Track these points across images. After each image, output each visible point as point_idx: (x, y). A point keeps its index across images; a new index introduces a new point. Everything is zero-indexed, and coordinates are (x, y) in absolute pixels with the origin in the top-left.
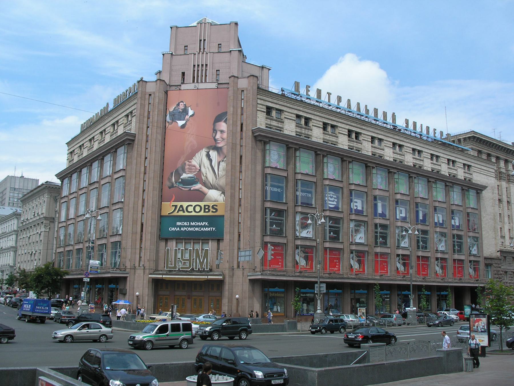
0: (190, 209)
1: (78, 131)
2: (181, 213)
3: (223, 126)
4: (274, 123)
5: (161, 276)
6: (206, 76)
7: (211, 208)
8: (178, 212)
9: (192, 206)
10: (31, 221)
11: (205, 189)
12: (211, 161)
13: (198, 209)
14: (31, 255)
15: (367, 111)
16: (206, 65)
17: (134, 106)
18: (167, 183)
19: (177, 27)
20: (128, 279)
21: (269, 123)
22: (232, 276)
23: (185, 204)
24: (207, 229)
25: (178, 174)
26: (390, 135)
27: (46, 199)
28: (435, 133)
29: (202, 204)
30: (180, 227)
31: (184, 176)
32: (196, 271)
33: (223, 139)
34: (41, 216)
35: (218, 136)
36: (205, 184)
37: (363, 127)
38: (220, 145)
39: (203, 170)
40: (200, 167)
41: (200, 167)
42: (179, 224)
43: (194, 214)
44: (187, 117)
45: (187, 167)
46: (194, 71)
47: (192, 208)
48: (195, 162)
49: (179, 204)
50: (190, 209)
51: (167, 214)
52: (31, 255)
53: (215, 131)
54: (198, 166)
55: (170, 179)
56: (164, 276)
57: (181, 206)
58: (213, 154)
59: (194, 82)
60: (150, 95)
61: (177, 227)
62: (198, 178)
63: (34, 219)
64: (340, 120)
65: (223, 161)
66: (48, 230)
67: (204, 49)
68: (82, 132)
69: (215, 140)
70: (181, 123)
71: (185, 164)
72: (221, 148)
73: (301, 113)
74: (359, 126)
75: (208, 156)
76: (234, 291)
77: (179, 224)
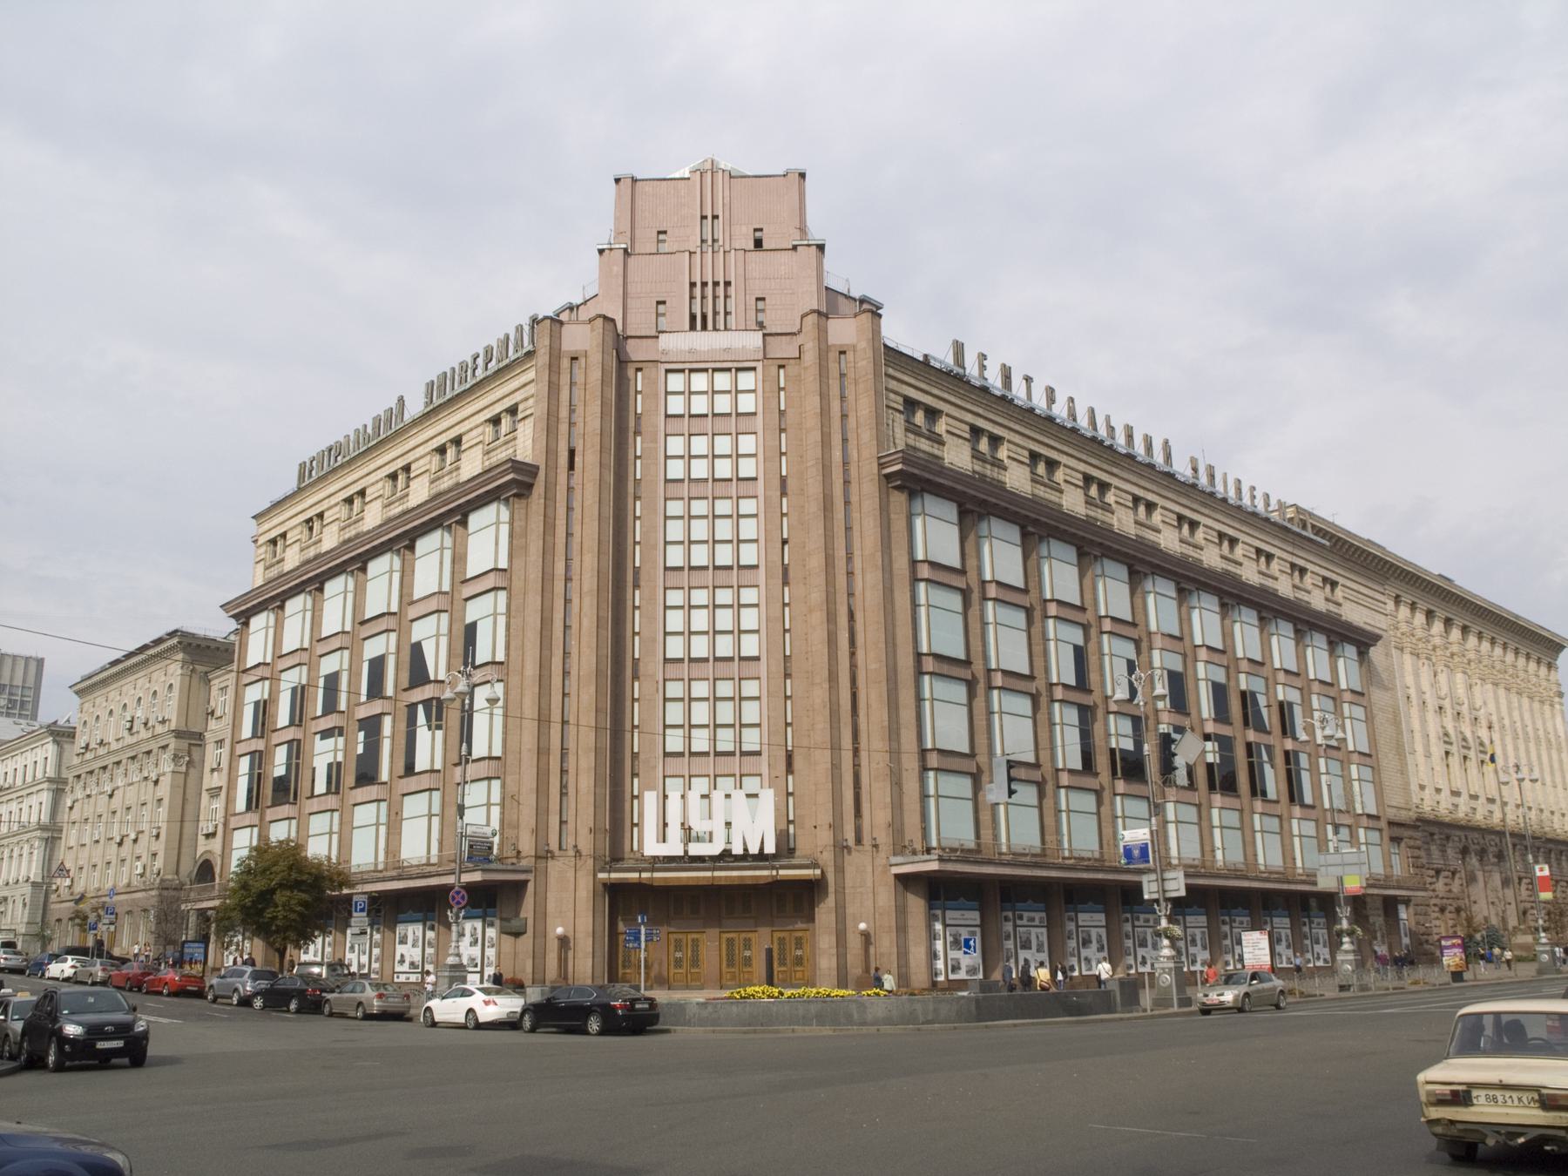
1: (291, 485)
4: (924, 445)
5: (636, 875)
10: (114, 746)
14: (120, 844)
15: (1111, 429)
17: (526, 387)
19: (634, 180)
20: (531, 886)
21: (911, 442)
22: (840, 870)
26: (1170, 495)
27: (176, 682)
28: (1253, 497)
32: (737, 858)
34: (159, 729)
37: (1115, 470)
46: (692, 297)
52: (120, 844)
56: (644, 875)
59: (693, 327)
60: (574, 359)
63: (129, 740)
64: (1065, 449)
66: (183, 769)
68: (300, 490)
73: (981, 423)
74: (1105, 466)
76: (850, 910)
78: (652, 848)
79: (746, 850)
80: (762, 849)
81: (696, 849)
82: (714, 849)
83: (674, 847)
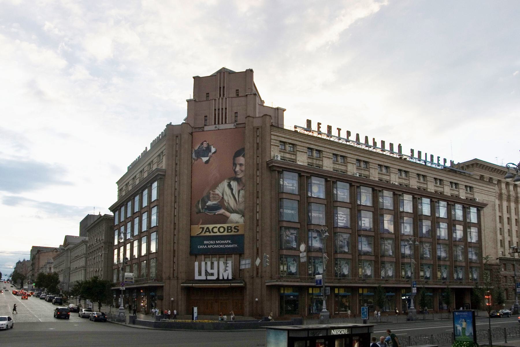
0: (216, 230)
2: (208, 234)
3: (241, 160)
6: (226, 118)
7: (233, 229)
8: (205, 233)
9: (216, 227)
11: (227, 214)
12: (232, 190)
13: (222, 230)
16: (226, 109)
18: (195, 210)
23: (211, 226)
24: (230, 246)
25: (204, 202)
29: (225, 226)
30: (207, 245)
31: (209, 203)
32: (221, 280)
33: (242, 171)
35: (238, 168)
36: (228, 210)
38: (239, 176)
39: (225, 198)
40: (223, 195)
41: (223, 195)
42: (205, 242)
43: (218, 234)
44: (210, 154)
45: (211, 196)
46: (215, 114)
47: (216, 229)
48: (218, 191)
49: (206, 226)
50: (216, 230)
51: (196, 235)
53: (235, 165)
54: (221, 195)
55: (197, 206)
57: (208, 228)
58: (234, 184)
59: (215, 124)
60: (177, 136)
61: (204, 245)
62: (221, 204)
65: (242, 189)
67: (224, 95)
69: (236, 172)
70: (205, 159)
71: (210, 193)
72: (240, 178)
75: (229, 186)
77: (205, 242)
78: (197, 277)
79: (223, 278)
80: (228, 278)
81: (209, 278)
82: (215, 277)
83: (203, 277)
